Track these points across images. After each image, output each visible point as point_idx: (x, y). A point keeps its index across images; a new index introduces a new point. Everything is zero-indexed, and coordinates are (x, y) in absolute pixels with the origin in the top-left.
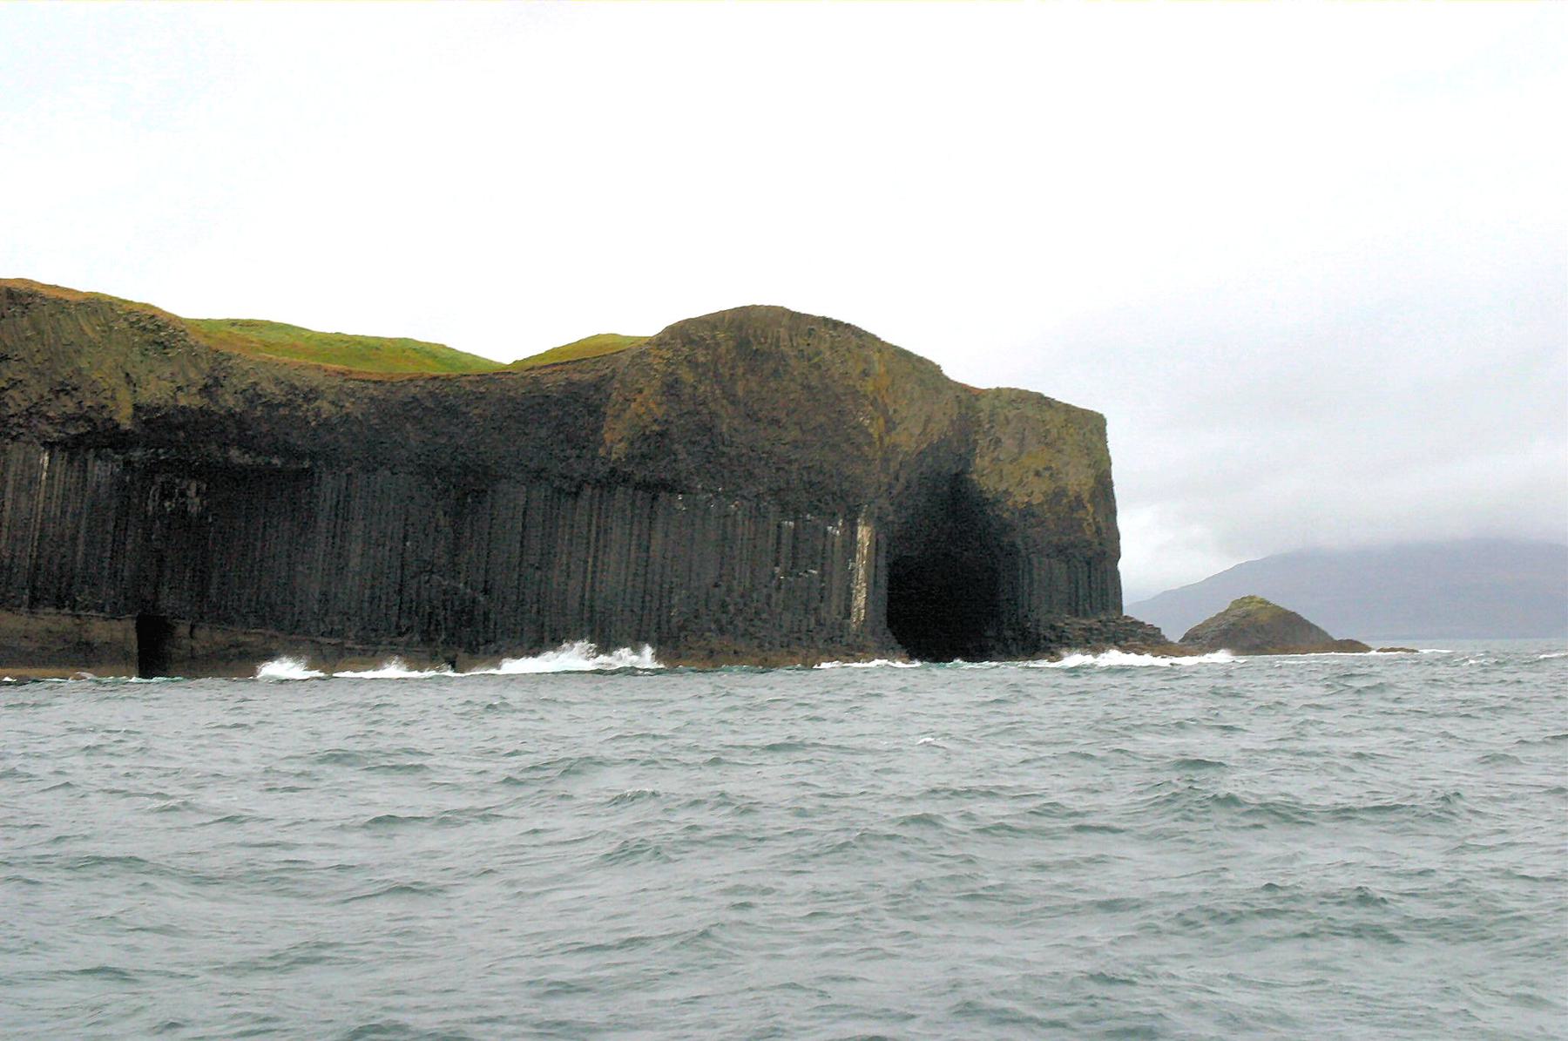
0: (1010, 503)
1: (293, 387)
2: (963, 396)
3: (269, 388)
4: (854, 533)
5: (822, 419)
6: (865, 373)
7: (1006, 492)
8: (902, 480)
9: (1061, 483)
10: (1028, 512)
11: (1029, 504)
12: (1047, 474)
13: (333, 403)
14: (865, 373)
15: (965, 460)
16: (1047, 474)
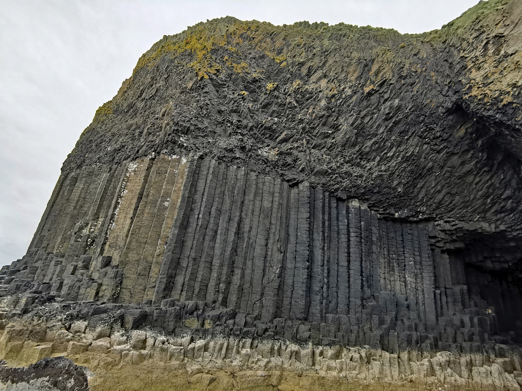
8: (344, 127)
15: (455, 87)
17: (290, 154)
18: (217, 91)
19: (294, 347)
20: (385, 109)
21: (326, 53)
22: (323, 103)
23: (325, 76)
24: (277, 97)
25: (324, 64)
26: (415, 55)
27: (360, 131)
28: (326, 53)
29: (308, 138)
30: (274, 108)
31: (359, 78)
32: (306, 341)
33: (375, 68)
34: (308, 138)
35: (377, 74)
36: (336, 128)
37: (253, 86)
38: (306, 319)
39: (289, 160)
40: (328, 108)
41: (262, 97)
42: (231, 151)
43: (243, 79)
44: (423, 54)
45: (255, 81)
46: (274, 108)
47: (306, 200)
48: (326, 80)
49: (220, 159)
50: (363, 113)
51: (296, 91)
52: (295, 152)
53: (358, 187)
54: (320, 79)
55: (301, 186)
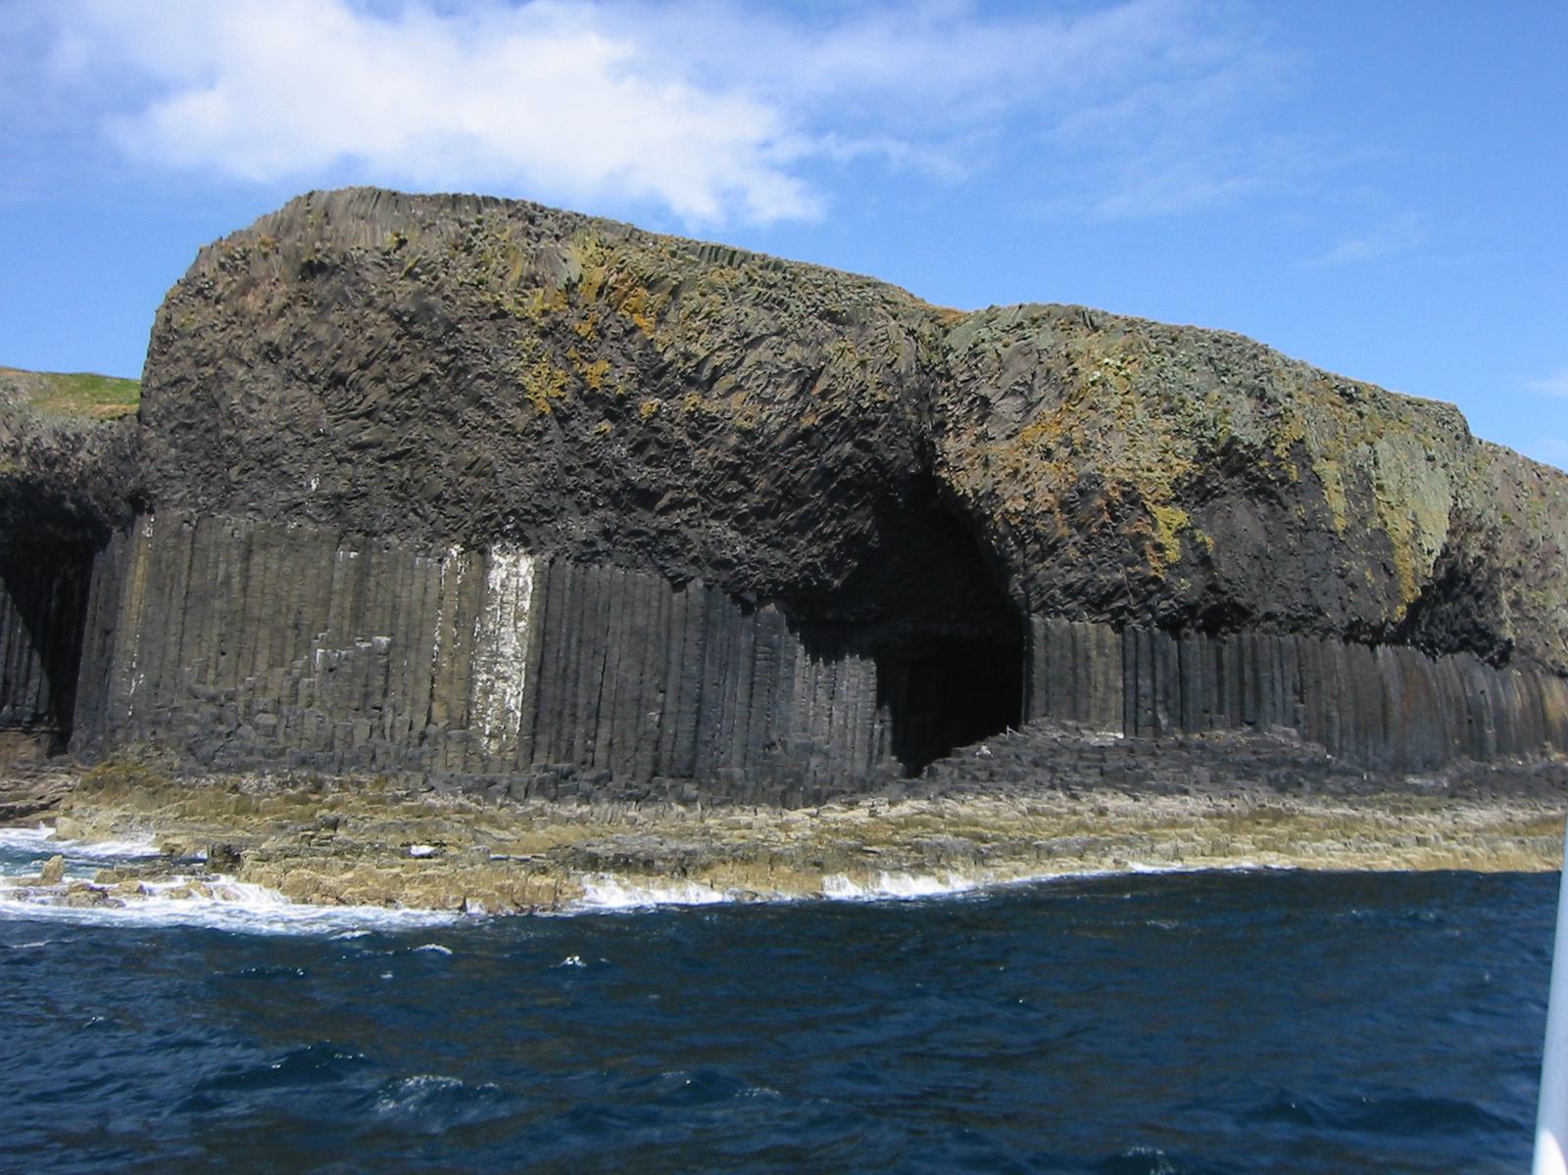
0: (997, 517)
1: (65, 438)
2: (926, 329)
3: (48, 442)
4: (487, 566)
5: (427, 368)
6: (532, 281)
7: (992, 494)
8: (763, 484)
9: (1089, 467)
10: (1025, 528)
11: (1028, 518)
12: (1064, 452)
13: (89, 452)
14: (532, 281)
15: (925, 451)
16: (1064, 452)
17: (674, 533)
18: (563, 428)
19: (681, 809)
20: (828, 459)
21: (746, 340)
22: (733, 440)
23: (739, 387)
24: (658, 430)
25: (740, 363)
26: (890, 366)
27: (790, 496)
28: (746, 340)
29: (705, 501)
30: (652, 451)
31: (795, 398)
32: (694, 801)
33: (822, 384)
34: (705, 501)
35: (823, 395)
36: (750, 486)
37: (618, 408)
38: (691, 776)
39: (673, 543)
40: (738, 451)
41: (634, 430)
42: (592, 544)
43: (602, 399)
44: (902, 367)
45: (622, 399)
46: (652, 451)
47: (698, 611)
48: (741, 395)
49: (577, 559)
50: (796, 462)
51: (690, 415)
52: (683, 528)
53: (775, 583)
54: (732, 390)
55: (691, 587)
